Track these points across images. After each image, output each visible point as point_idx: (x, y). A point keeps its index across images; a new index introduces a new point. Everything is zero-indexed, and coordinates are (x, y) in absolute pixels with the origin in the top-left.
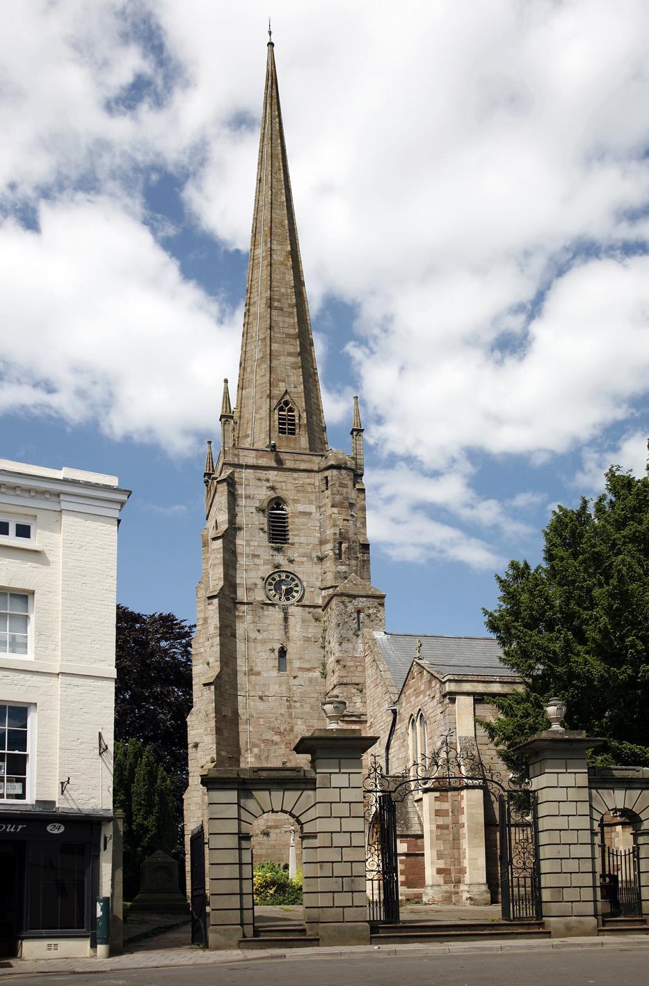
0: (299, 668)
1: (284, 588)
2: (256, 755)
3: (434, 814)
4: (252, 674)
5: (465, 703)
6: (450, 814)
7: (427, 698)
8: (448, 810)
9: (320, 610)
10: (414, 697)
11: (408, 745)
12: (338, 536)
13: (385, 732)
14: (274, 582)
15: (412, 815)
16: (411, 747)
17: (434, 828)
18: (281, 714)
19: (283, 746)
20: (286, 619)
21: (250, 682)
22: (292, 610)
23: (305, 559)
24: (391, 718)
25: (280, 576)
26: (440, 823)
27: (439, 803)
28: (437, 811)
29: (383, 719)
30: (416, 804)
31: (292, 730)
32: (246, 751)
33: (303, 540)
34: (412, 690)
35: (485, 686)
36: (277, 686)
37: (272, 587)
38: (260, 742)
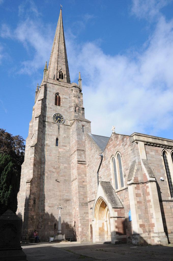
1: (59, 119)
3: (135, 196)
4: (47, 146)
5: (141, 144)
6: (142, 196)
7: (121, 146)
11: (110, 169)
12: (75, 105)
14: (56, 117)
15: (117, 199)
17: (136, 203)
19: (56, 174)
20: (59, 129)
25: (58, 115)
26: (138, 200)
27: (136, 190)
28: (136, 194)
30: (116, 193)
31: (59, 167)
33: (65, 106)
37: (55, 118)
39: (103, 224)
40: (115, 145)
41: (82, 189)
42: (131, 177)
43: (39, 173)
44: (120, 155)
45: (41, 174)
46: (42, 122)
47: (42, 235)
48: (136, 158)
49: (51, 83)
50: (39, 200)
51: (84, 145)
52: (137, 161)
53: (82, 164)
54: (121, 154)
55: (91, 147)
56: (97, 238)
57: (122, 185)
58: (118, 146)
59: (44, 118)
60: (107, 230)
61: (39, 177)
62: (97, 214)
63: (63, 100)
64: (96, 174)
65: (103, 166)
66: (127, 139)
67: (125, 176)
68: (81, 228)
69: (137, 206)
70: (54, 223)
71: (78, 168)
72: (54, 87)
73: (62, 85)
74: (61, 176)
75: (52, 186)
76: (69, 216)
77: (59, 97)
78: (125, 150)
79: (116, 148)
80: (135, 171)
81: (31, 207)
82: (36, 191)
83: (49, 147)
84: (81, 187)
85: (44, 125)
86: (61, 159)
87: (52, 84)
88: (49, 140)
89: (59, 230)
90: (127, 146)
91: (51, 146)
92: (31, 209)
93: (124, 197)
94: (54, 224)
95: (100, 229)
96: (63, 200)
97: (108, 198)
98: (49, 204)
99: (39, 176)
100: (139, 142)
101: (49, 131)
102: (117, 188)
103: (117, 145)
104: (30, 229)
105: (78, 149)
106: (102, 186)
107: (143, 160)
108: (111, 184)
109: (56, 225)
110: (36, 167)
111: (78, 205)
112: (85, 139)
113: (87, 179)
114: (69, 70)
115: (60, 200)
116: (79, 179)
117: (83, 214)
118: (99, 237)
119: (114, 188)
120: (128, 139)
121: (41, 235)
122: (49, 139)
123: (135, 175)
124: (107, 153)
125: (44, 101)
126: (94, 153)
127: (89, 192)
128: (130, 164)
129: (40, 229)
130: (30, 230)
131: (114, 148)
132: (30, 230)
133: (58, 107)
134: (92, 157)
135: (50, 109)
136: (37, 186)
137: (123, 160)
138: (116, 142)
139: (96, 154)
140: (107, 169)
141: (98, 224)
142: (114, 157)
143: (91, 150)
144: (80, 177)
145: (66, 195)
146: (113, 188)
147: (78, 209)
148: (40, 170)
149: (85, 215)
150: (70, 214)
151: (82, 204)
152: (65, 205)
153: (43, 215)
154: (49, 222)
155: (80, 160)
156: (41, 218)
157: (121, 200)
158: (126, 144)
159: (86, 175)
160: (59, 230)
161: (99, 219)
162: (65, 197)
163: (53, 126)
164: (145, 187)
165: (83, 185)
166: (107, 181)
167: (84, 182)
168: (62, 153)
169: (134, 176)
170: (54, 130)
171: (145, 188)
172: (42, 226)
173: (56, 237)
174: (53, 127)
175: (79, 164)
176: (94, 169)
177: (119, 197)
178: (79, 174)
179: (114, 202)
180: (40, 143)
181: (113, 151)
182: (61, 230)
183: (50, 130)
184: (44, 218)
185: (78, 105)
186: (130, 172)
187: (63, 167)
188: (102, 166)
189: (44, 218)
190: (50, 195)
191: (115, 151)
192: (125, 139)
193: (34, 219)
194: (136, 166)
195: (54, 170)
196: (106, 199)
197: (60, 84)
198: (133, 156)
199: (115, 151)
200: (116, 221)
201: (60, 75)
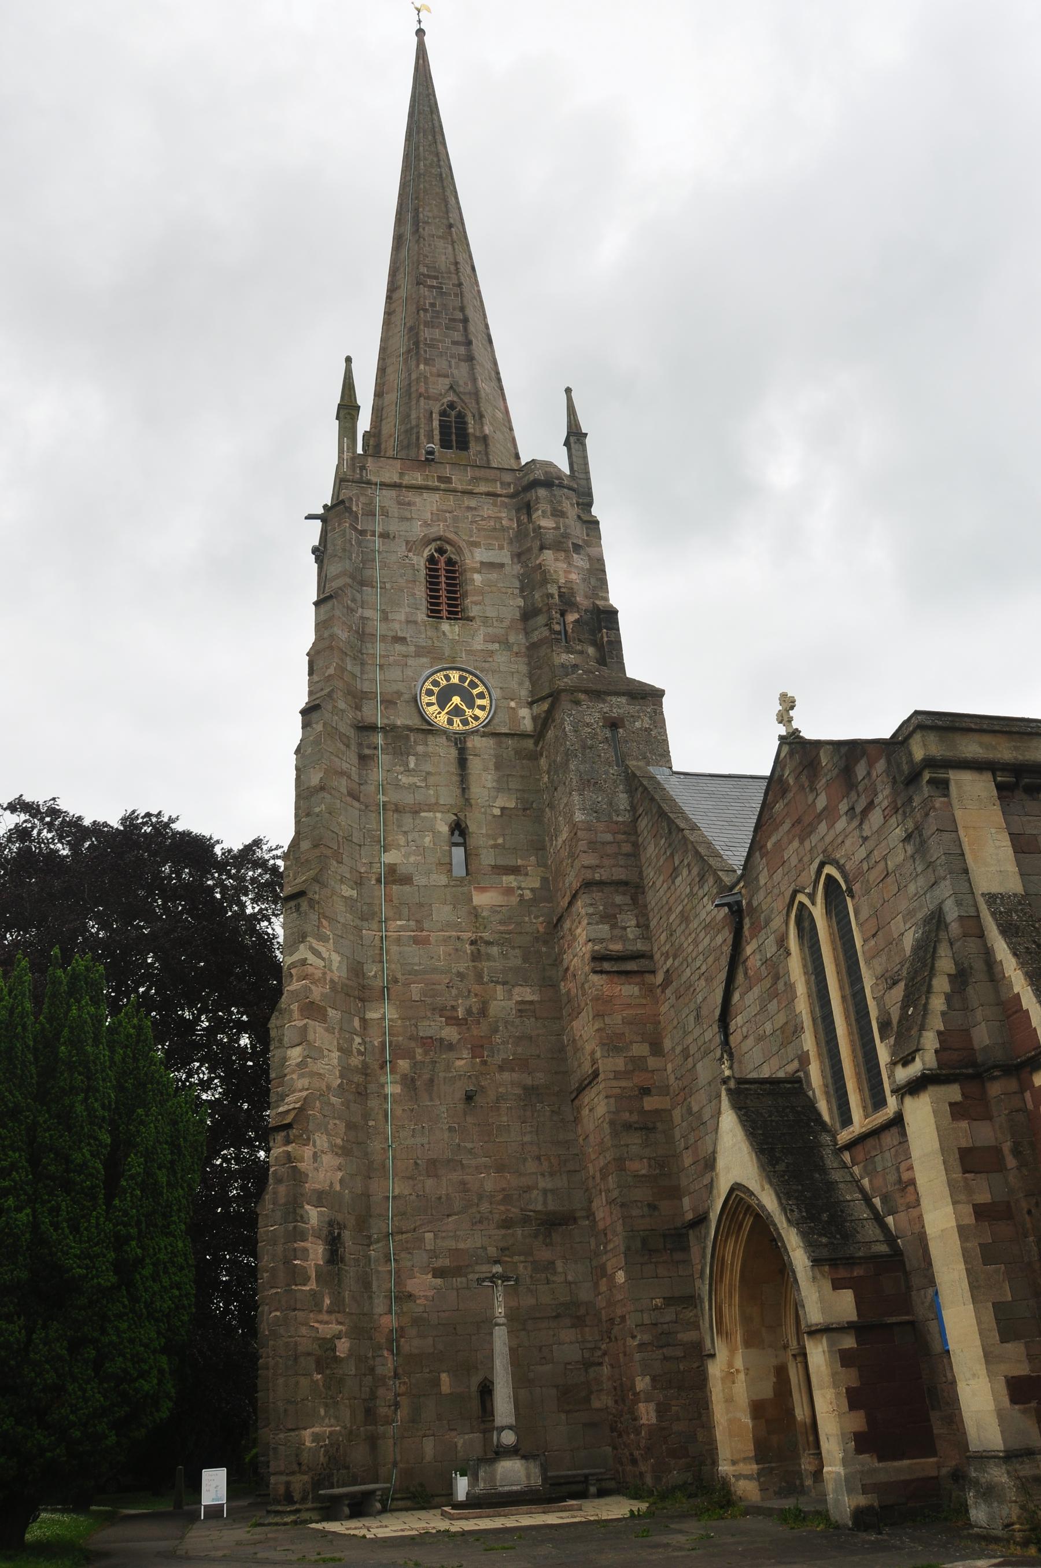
0: (495, 867)
1: (456, 700)
2: (404, 1077)
3: (959, 1169)
4: (394, 882)
6: (1011, 1162)
7: (841, 824)
8: (997, 1150)
9: (530, 744)
10: (796, 844)
11: (790, 987)
13: (709, 980)
14: (436, 690)
15: (851, 1196)
16: (801, 989)
17: (970, 1220)
18: (460, 975)
19: (466, 1054)
20: (462, 762)
21: (389, 899)
22: (475, 743)
23: (496, 646)
24: (724, 938)
25: (447, 678)
26: (984, 1197)
27: (964, 1124)
29: (701, 948)
30: (847, 1157)
31: (483, 1012)
32: (383, 1066)
33: (491, 612)
34: (786, 826)
35: (1016, 748)
36: (448, 908)
37: (433, 699)
38: (413, 1044)
39: (781, 1372)
40: (807, 820)
41: (634, 1141)
42: (914, 1032)
43: (355, 1061)
44: (844, 887)
45: (365, 1065)
46: (351, 733)
47: (401, 1465)
48: (945, 889)
49: (387, 480)
50: (369, 1237)
51: (627, 848)
52: (951, 913)
53: (627, 973)
54: (846, 882)
55: (672, 855)
56: (747, 1477)
57: (878, 1101)
58: (823, 827)
59: (358, 708)
60: (807, 1412)
61: (358, 1085)
62: (732, 1313)
63: (477, 577)
64: (712, 1034)
65: (751, 973)
66: (871, 765)
67: (885, 1026)
68: (652, 1406)
69: (973, 1244)
70: (475, 1381)
71: (603, 1006)
72: (409, 504)
73: (460, 487)
74: (501, 1069)
75: (446, 1135)
76: (573, 1326)
77: (450, 562)
78: (871, 843)
79: (814, 839)
80: (941, 984)
81: (312, 1285)
82: (341, 1181)
83: (407, 888)
84: (628, 1127)
85: (367, 752)
86: (489, 957)
87: (392, 493)
88: (402, 842)
89: (502, 1429)
90: (876, 817)
91: (420, 880)
92: (315, 1297)
93: (892, 1178)
94: (474, 1388)
95: (757, 1409)
96: (525, 1220)
97: (784, 1195)
98: (434, 1254)
99: (358, 1078)
100: (954, 776)
101: (398, 786)
102: (846, 1120)
103: (819, 817)
104: (316, 1429)
105: (588, 875)
106: (738, 1107)
107: (991, 899)
108: (810, 1093)
110: (325, 1021)
111: (622, 1249)
112: (633, 808)
113: (669, 1067)
114: (502, 389)
115: (507, 1224)
116: (612, 1076)
117: (657, 1308)
118: (755, 1467)
119: (826, 1117)
120: (881, 766)
121: (395, 1464)
122: (402, 842)
123: (943, 1014)
124: (762, 882)
125: (354, 600)
126: (692, 895)
127: (687, 1160)
128: (908, 942)
129: (388, 1422)
130: (316, 1438)
131: (802, 842)
132: (316, 1438)
133: (445, 626)
134: (685, 918)
135: (398, 647)
136: (343, 1148)
137: (863, 917)
138: (810, 802)
139: (705, 899)
140: (773, 994)
141: (742, 1376)
142: (806, 901)
143: (675, 872)
144: (619, 1063)
145: (545, 1192)
146: (823, 1124)
147: (620, 1277)
148: (358, 1040)
149: (669, 1315)
150: (582, 1311)
151: (644, 1241)
152: (544, 1254)
154: (444, 1377)
155: (612, 947)
156: (386, 1353)
157: (877, 1201)
158: (871, 805)
159: (656, 1048)
161: (748, 1344)
162: (541, 1199)
163: (420, 749)
164: (1028, 1095)
165: (642, 1112)
166: (781, 1074)
167: (646, 1091)
168: (498, 917)
169: (936, 1023)
170: (432, 780)
171: (1030, 1106)
172: (397, 1405)
173: (481, 1474)
174: (426, 755)
175: (607, 973)
176: (700, 998)
177: (866, 1182)
178: (613, 1044)
179: (825, 1216)
180: (344, 870)
181: (794, 861)
182: (510, 1428)
183: (404, 780)
184: (406, 1348)
185: (573, 594)
186: (908, 1001)
187: (511, 1004)
188: (746, 974)
189: (406, 1348)
190: (440, 1198)
191: (806, 859)
192: (861, 770)
193: (337, 1360)
194: (944, 950)
195: (450, 1033)
196: (769, 1200)
197: (448, 480)
198: (921, 881)
199: (806, 859)
200: (846, 1358)
201: (444, 428)
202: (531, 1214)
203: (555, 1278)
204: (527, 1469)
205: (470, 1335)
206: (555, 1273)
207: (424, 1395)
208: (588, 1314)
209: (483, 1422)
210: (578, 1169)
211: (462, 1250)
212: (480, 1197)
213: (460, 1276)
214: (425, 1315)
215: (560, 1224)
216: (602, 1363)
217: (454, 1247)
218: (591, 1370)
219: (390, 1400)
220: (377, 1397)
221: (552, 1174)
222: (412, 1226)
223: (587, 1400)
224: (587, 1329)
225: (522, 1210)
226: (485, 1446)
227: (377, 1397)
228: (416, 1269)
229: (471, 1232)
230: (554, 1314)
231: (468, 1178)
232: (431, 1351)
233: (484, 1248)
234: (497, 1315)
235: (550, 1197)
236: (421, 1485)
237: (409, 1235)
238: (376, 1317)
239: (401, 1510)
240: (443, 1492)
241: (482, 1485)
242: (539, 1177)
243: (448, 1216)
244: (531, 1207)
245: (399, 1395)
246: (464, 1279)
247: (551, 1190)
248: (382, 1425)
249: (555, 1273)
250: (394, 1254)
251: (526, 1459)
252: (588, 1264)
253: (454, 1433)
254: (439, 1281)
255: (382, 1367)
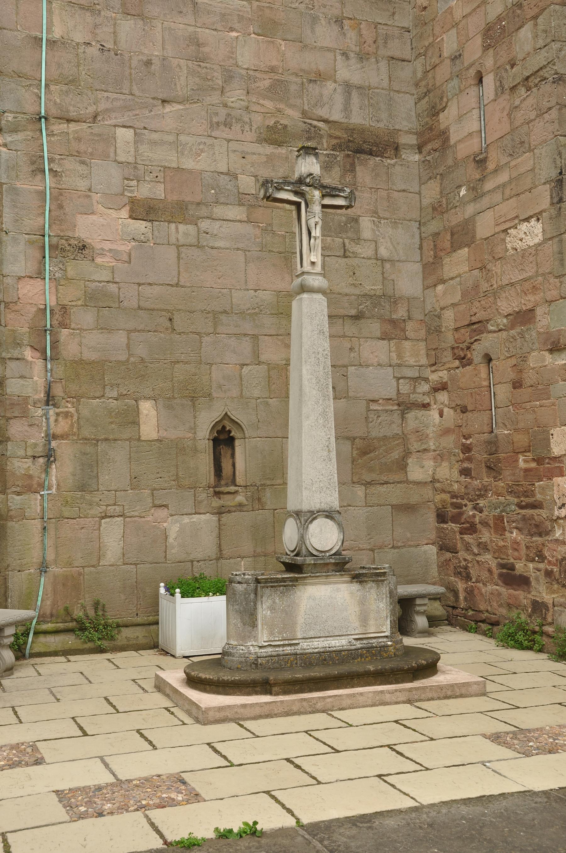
47: (54, 570)
89: (313, 515)
109: (230, 441)
121: (43, 568)
145: (348, 87)
150: (401, 313)
153: (64, 309)
156: (28, 354)
160: (313, 515)
162: (339, 99)
190: (148, 63)
202: (321, 124)
203: (358, 249)
204: (362, 602)
205: (198, 334)
206: (357, 240)
207: (106, 440)
208: (409, 318)
209: (217, 494)
210: (408, 57)
211: (190, 172)
212: (229, 77)
213: (184, 221)
214: (113, 288)
215: (371, 153)
216: (428, 404)
217: (174, 165)
218: (411, 415)
219: (35, 445)
220: (8, 439)
221: (362, 57)
222: (91, 110)
223: (402, 465)
224: (407, 344)
225: (304, 114)
226: (219, 537)
227: (8, 439)
228: (96, 197)
229: (209, 141)
230: (353, 312)
231: (205, 34)
232: (123, 358)
233: (233, 176)
234: (307, 267)
235: (355, 94)
236: (96, 605)
237: (85, 126)
238: (9, 281)
239: (55, 654)
240: (139, 620)
241: (263, 637)
242: (339, 57)
243: (164, 101)
244: (323, 112)
245: (55, 437)
246: (191, 229)
247: (359, 88)
248: (19, 494)
249: (357, 240)
250: (51, 160)
251: (361, 582)
252: (417, 232)
253: (162, 513)
254: (141, 226)
255: (21, 381)
